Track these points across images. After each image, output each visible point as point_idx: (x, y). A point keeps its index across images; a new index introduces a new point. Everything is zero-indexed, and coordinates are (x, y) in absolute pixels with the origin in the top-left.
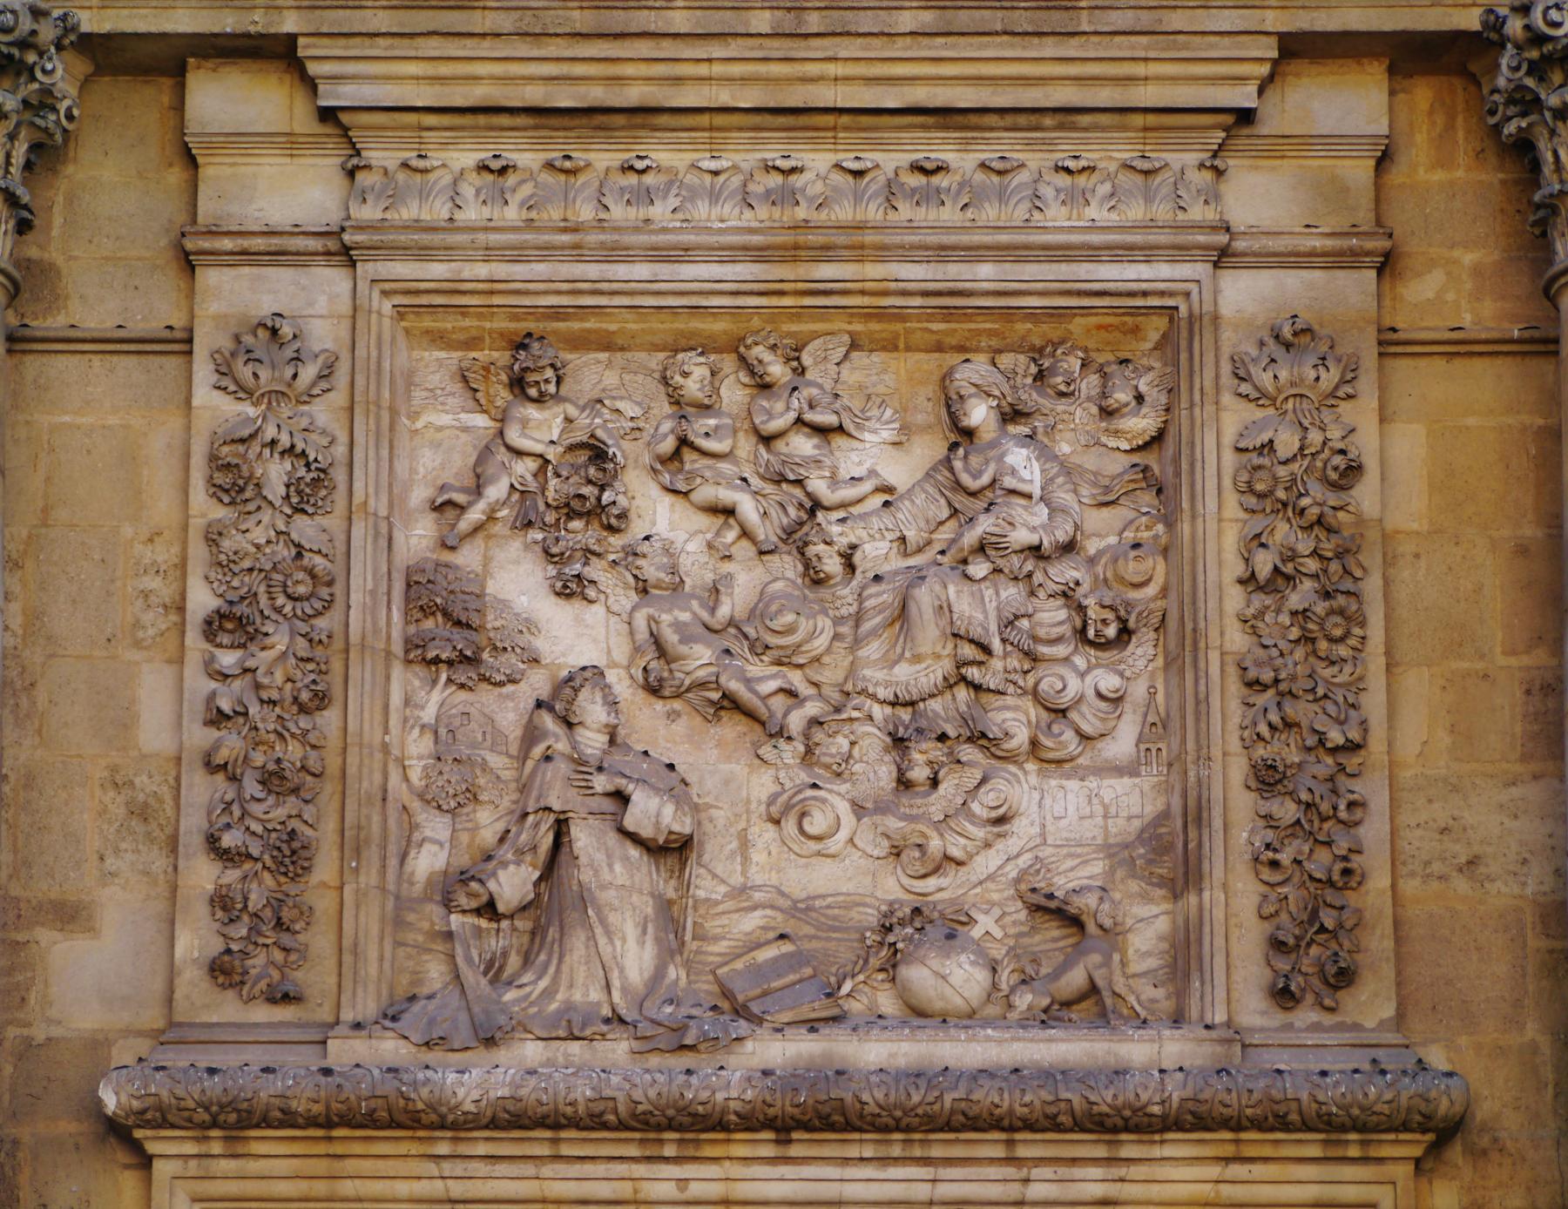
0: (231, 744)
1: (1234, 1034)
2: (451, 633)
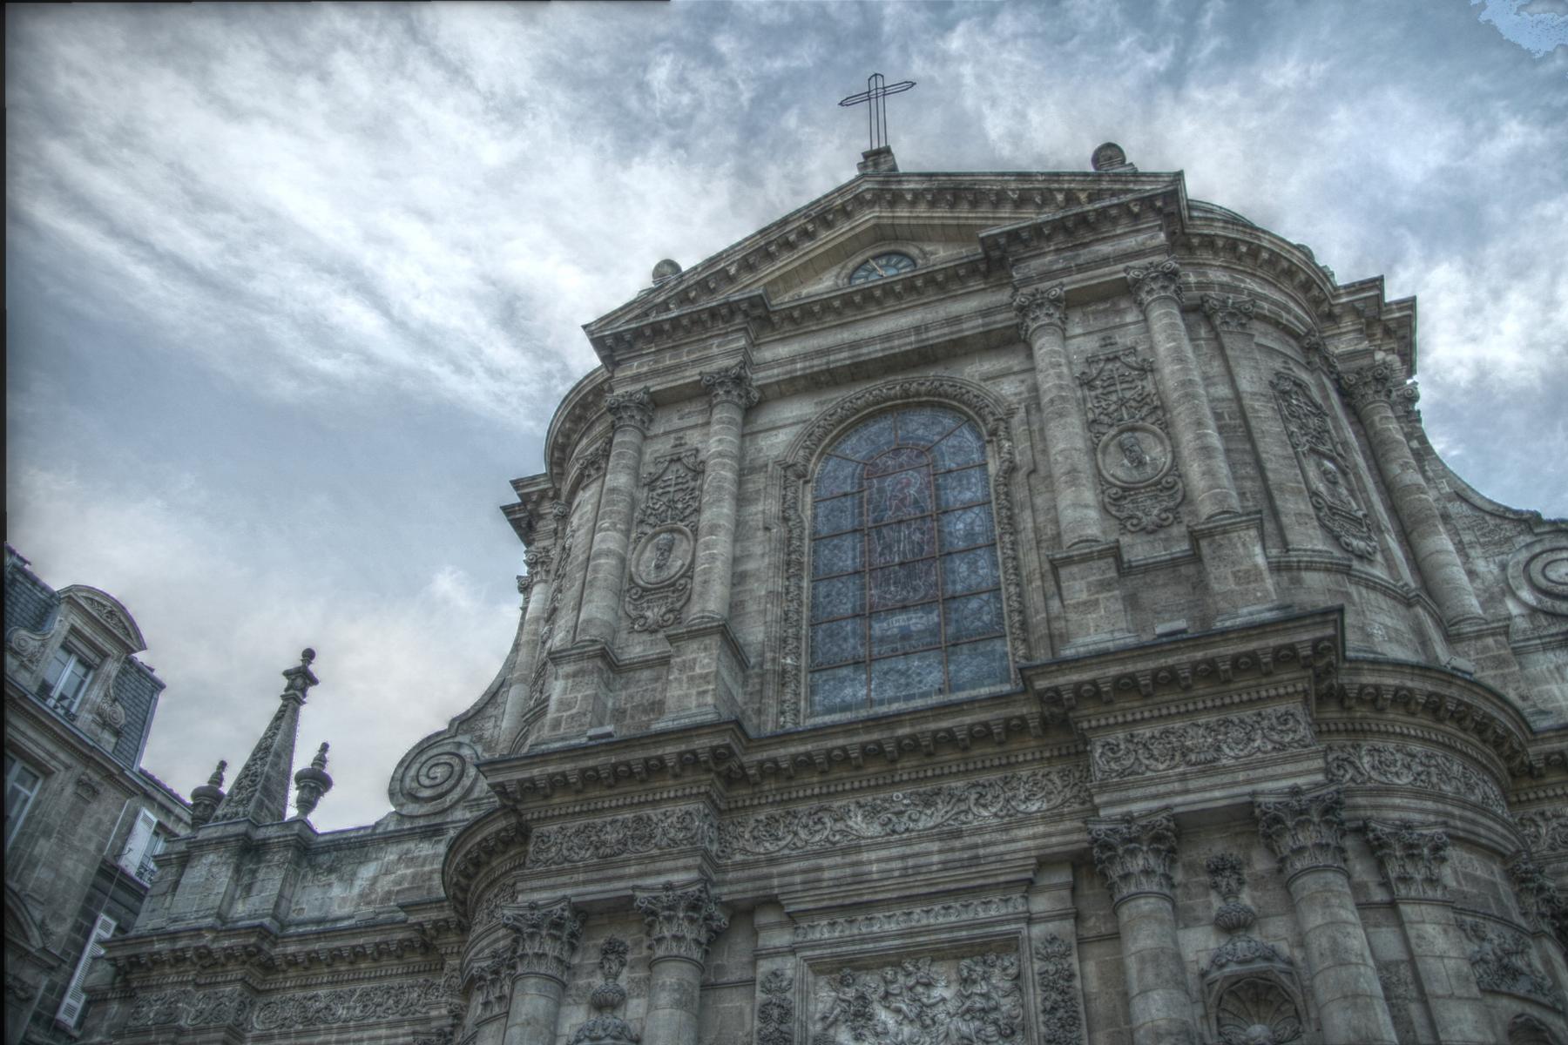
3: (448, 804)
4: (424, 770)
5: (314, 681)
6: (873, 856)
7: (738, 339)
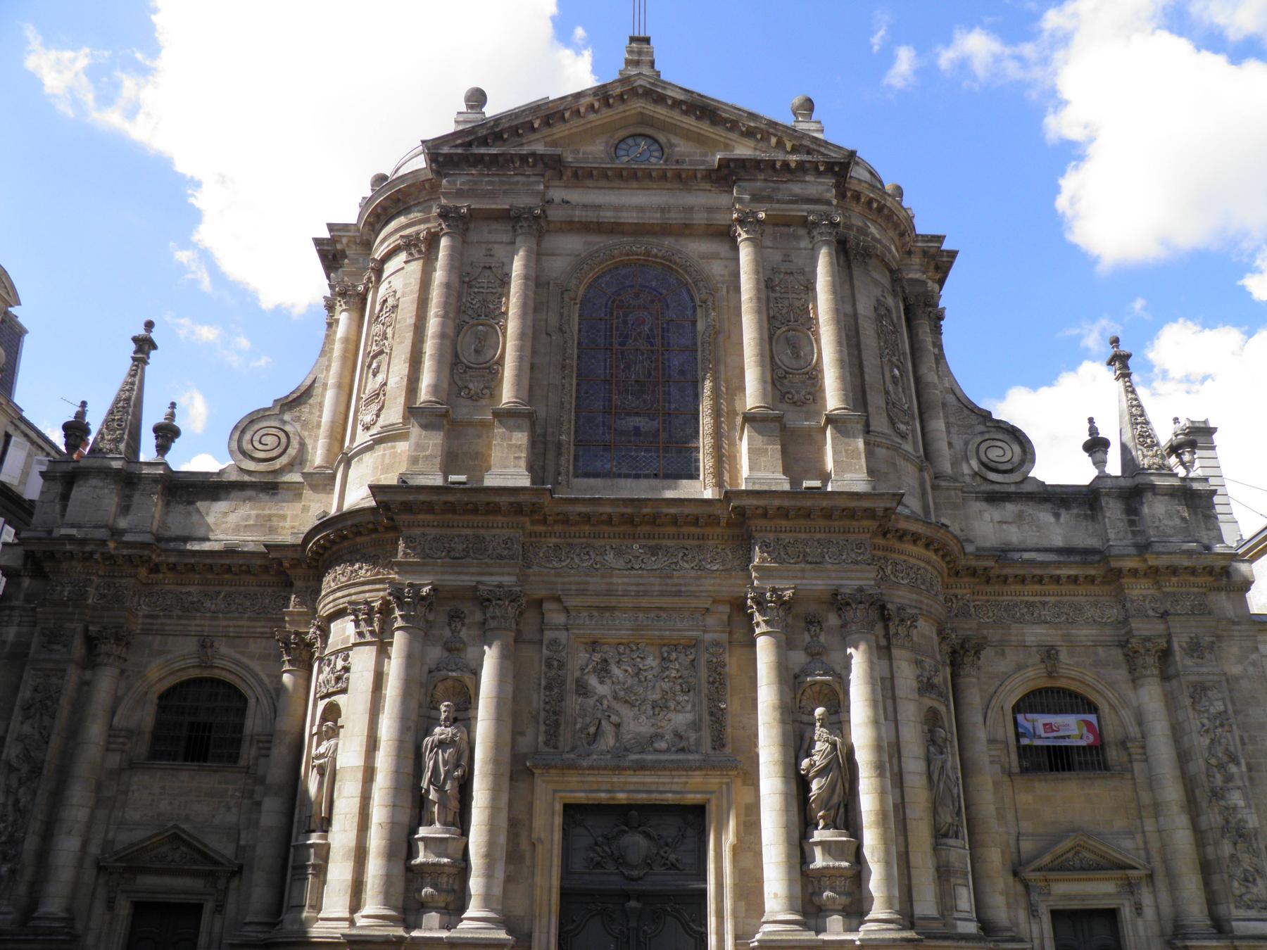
0: (548, 707)
1: (707, 755)
2: (582, 689)
3: (278, 467)
4: (257, 438)
5: (154, 347)
6: (620, 581)
7: (538, 183)
